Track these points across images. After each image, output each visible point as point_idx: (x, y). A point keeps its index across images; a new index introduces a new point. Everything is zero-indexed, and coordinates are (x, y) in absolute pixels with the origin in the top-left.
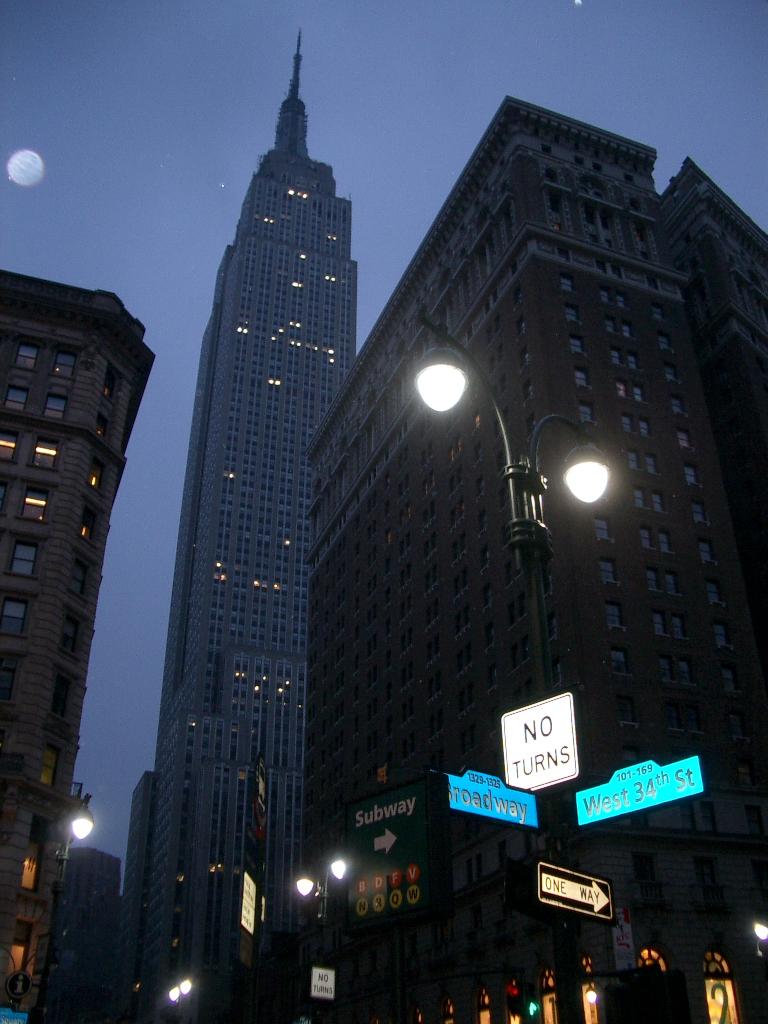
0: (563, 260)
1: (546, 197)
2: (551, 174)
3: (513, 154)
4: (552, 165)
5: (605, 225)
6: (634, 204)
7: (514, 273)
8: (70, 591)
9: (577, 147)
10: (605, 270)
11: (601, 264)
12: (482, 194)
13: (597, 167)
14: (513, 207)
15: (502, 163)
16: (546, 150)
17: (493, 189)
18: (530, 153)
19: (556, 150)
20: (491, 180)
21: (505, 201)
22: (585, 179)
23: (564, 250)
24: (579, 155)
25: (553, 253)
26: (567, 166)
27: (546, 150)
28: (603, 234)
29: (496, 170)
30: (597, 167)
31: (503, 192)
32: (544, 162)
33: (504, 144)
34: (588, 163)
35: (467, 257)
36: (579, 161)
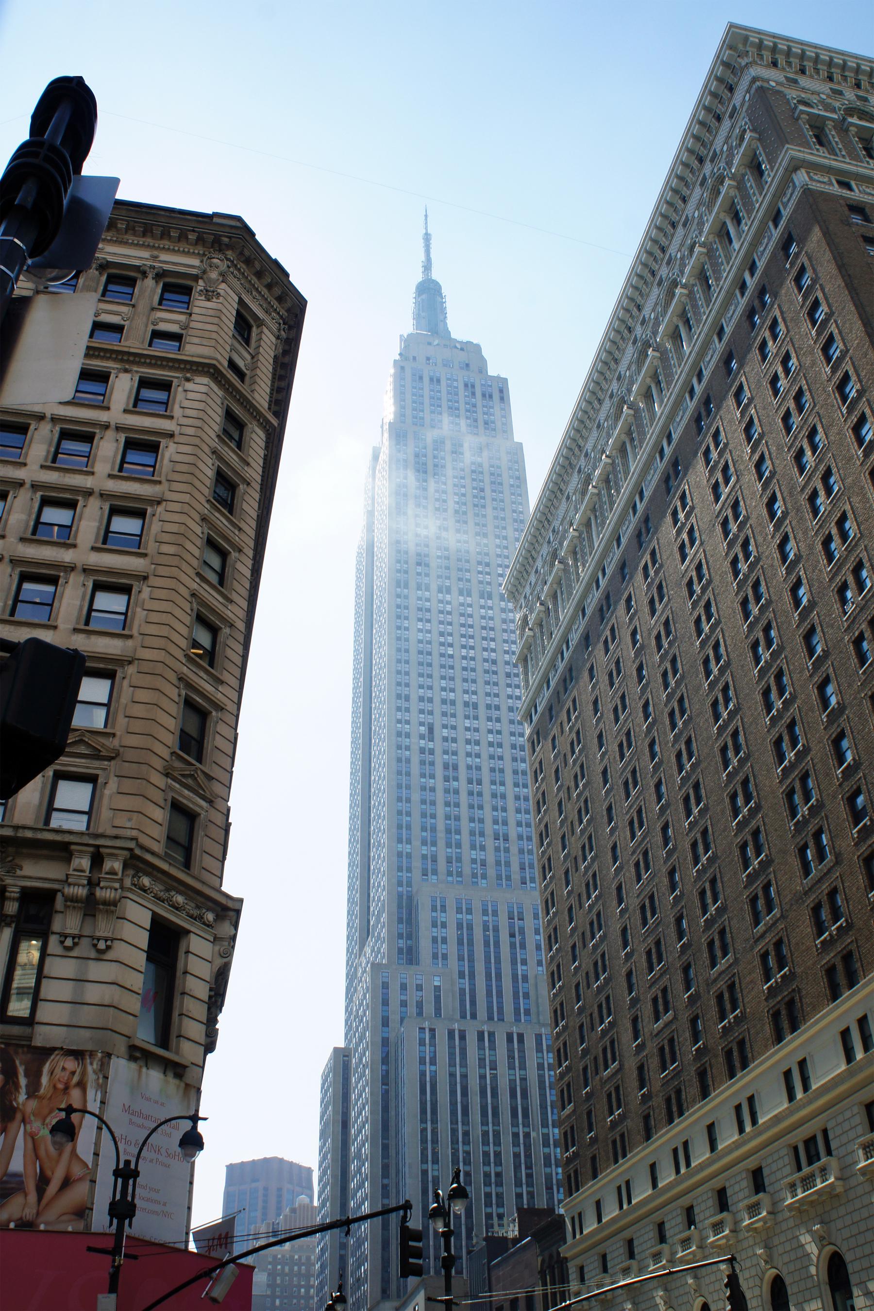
18: (773, 84)
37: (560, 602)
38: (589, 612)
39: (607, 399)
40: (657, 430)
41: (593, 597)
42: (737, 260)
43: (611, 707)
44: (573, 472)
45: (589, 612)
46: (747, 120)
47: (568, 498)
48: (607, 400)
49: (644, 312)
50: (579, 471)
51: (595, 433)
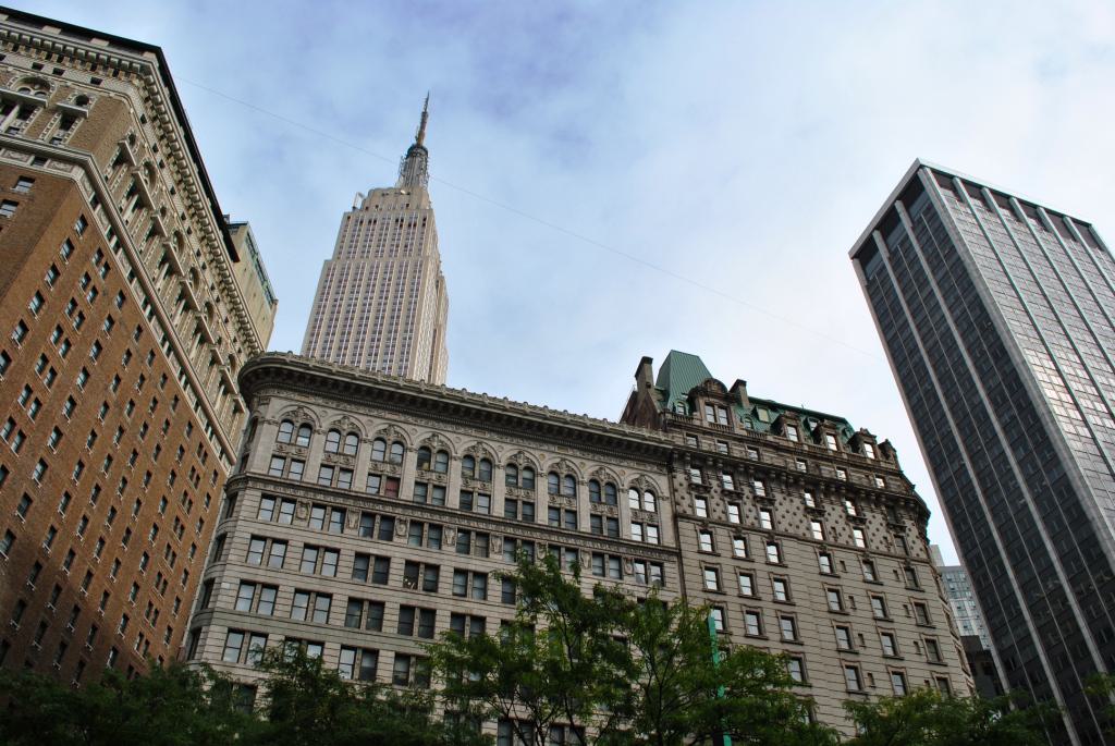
1: (116, 152)
2: (133, 139)
5: (133, 211)
6: (163, 211)
10: (110, 240)
11: (112, 233)
13: (162, 165)
16: (143, 120)
18: (132, 111)
19: (148, 127)
22: (148, 165)
26: (146, 145)
27: (143, 120)
28: (128, 215)
30: (162, 165)
32: (134, 128)
34: (159, 157)
36: (155, 150)
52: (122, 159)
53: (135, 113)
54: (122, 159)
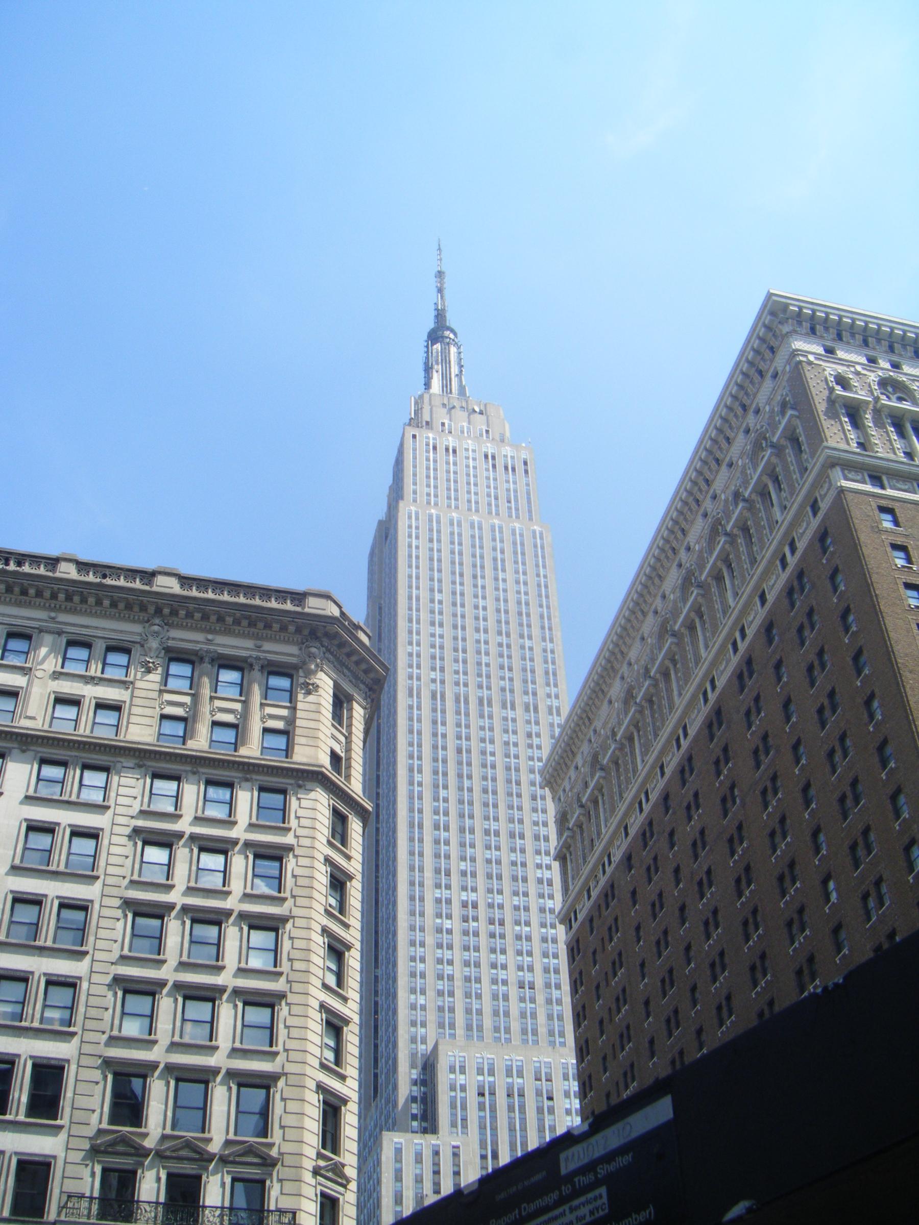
0: (878, 490)
2: (842, 381)
3: (788, 362)
4: (841, 369)
7: (815, 514)
8: (325, 986)
9: (866, 343)
12: (751, 419)
14: (800, 430)
15: (775, 376)
17: (767, 408)
18: (811, 358)
20: (761, 398)
21: (789, 421)
23: (876, 479)
24: (871, 353)
25: (864, 482)
27: (830, 351)
29: (768, 384)
31: (783, 413)
32: (830, 369)
33: (772, 350)
35: (745, 500)
37: (601, 810)
38: (632, 831)
39: (651, 615)
40: (701, 674)
41: (636, 818)
42: (779, 535)
43: (653, 939)
44: (615, 676)
45: (632, 831)
46: (787, 389)
47: (610, 702)
48: (651, 615)
49: (688, 539)
50: (622, 678)
51: (637, 645)
52: (854, 412)
53: (818, 356)
54: (854, 412)
